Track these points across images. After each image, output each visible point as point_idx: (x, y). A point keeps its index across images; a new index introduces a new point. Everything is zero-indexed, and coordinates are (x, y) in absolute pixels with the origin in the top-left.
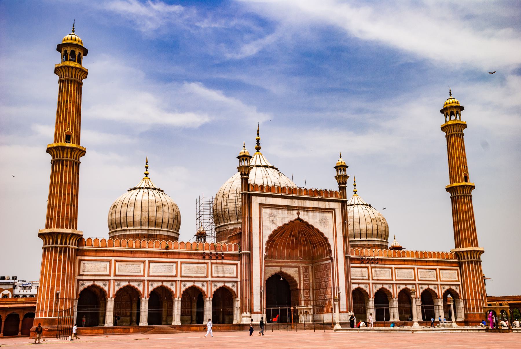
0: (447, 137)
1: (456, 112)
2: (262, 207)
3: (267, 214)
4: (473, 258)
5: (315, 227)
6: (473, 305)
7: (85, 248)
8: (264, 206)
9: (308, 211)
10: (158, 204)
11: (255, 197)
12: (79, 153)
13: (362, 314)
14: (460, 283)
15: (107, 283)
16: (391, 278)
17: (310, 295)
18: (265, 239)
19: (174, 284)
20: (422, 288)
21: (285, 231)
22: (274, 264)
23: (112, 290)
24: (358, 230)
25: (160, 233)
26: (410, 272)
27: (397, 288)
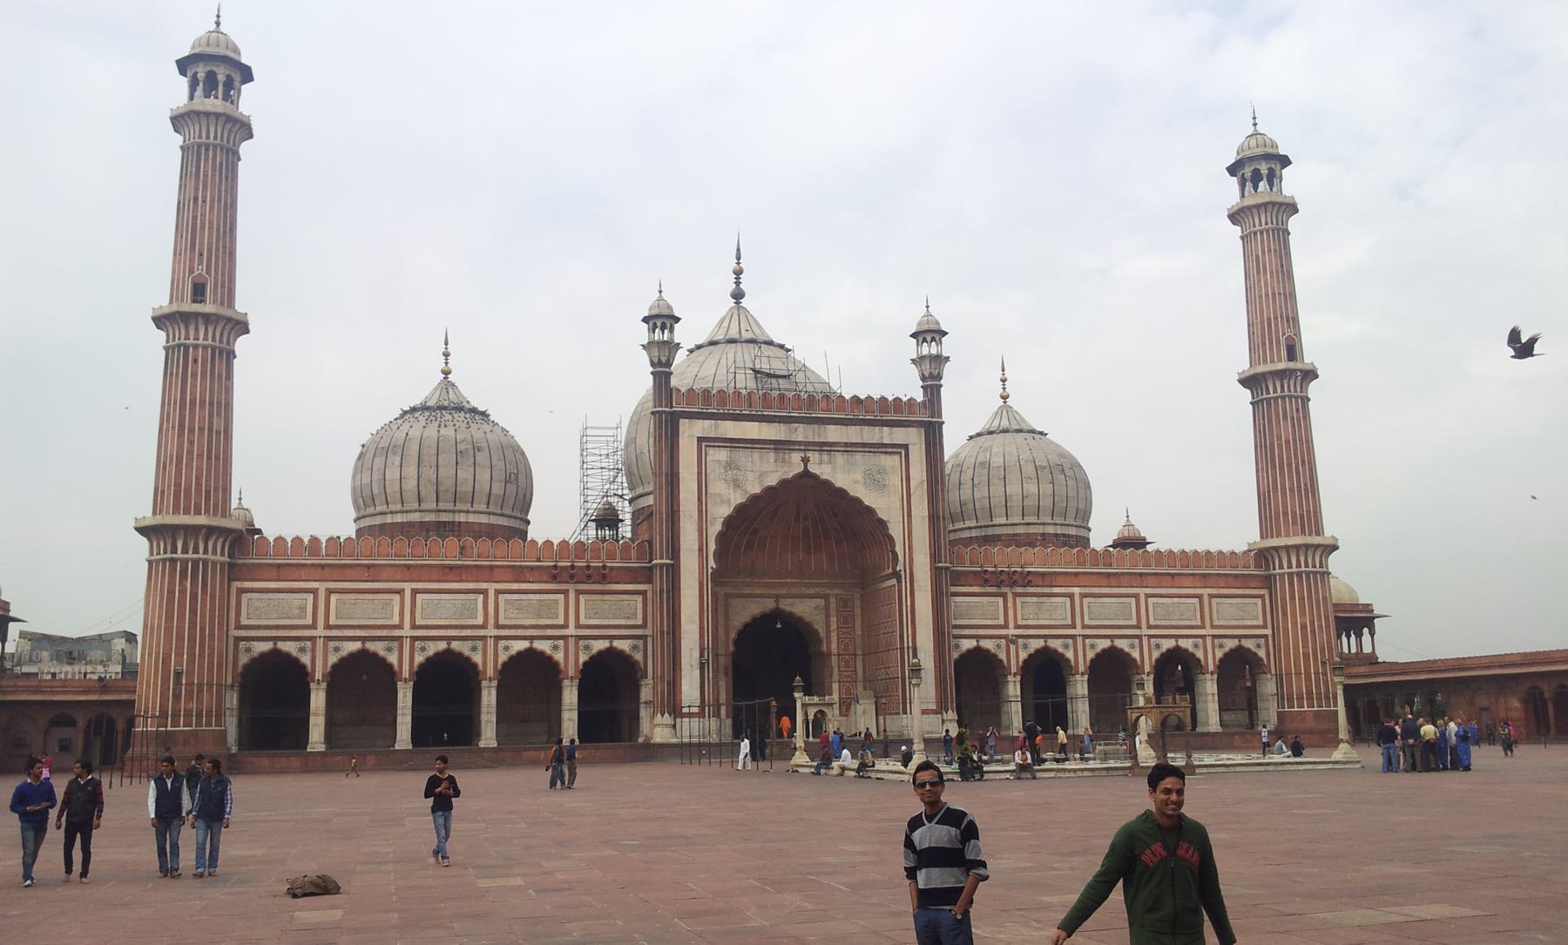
0: (1242, 238)
1: (1267, 171)
2: (706, 446)
3: (720, 464)
4: (1303, 565)
6: (1299, 687)
7: (251, 561)
10: (461, 447)
11: (687, 420)
12: (228, 327)
14: (1268, 632)
15: (309, 643)
17: (855, 667)
18: (715, 528)
19: (479, 644)
20: (1158, 646)
23: (319, 663)
24: (1000, 497)
26: (1124, 607)
27: (1088, 647)
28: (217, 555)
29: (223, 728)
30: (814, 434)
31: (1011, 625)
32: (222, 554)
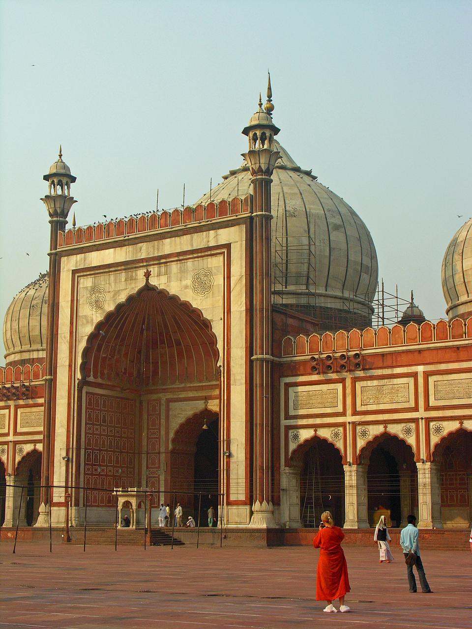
9: (168, 264)
10: (34, 302)
13: (452, 506)
16: (412, 404)
18: (82, 345)
21: (175, 319)
22: (191, 394)
25: (38, 354)
30: (154, 250)
31: (349, 411)
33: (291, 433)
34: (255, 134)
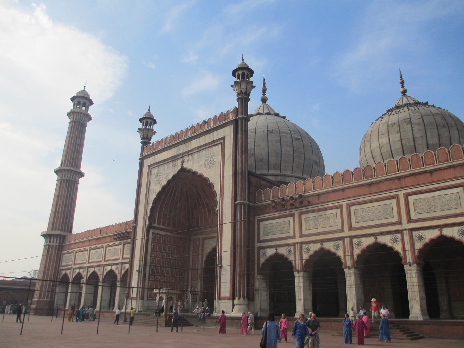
5: (200, 172)
8: (153, 167)
9: (193, 154)
11: (146, 159)
16: (339, 227)
18: (150, 205)
20: (421, 238)
23: (71, 278)
24: (369, 152)
27: (354, 245)
28: (55, 243)
29: (53, 300)
31: (297, 235)
32: (56, 243)
33: (261, 252)
34: (239, 74)
